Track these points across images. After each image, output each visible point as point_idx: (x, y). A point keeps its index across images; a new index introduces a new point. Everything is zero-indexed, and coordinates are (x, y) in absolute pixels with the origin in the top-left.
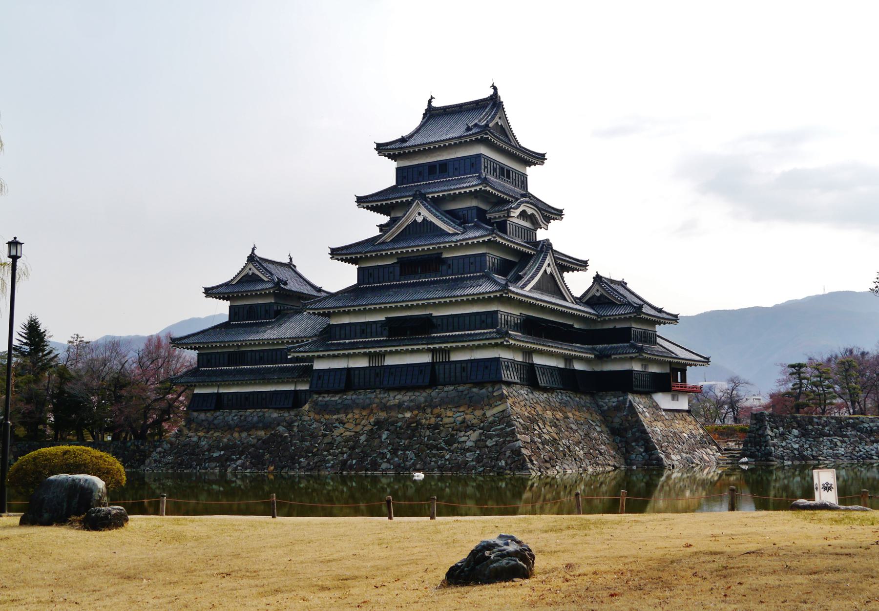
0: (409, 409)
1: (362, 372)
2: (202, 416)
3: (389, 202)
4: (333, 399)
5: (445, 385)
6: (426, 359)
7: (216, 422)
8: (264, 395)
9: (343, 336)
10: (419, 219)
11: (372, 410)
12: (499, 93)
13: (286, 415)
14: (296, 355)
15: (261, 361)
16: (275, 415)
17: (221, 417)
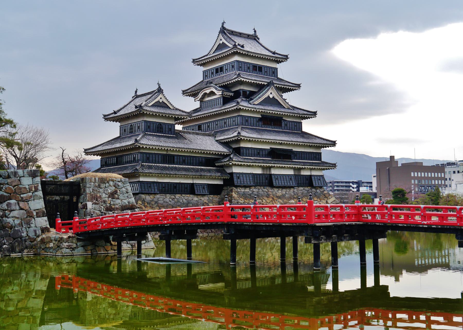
0: (290, 198)
1: (258, 176)
2: (148, 198)
3: (255, 82)
4: (246, 191)
5: (298, 186)
6: (291, 172)
7: (159, 202)
8: (186, 186)
9: (247, 154)
10: (271, 96)
11: (273, 199)
12: (257, 34)
13: (202, 199)
14: (234, 163)
15: (184, 163)
16: (196, 199)
17: (162, 199)
